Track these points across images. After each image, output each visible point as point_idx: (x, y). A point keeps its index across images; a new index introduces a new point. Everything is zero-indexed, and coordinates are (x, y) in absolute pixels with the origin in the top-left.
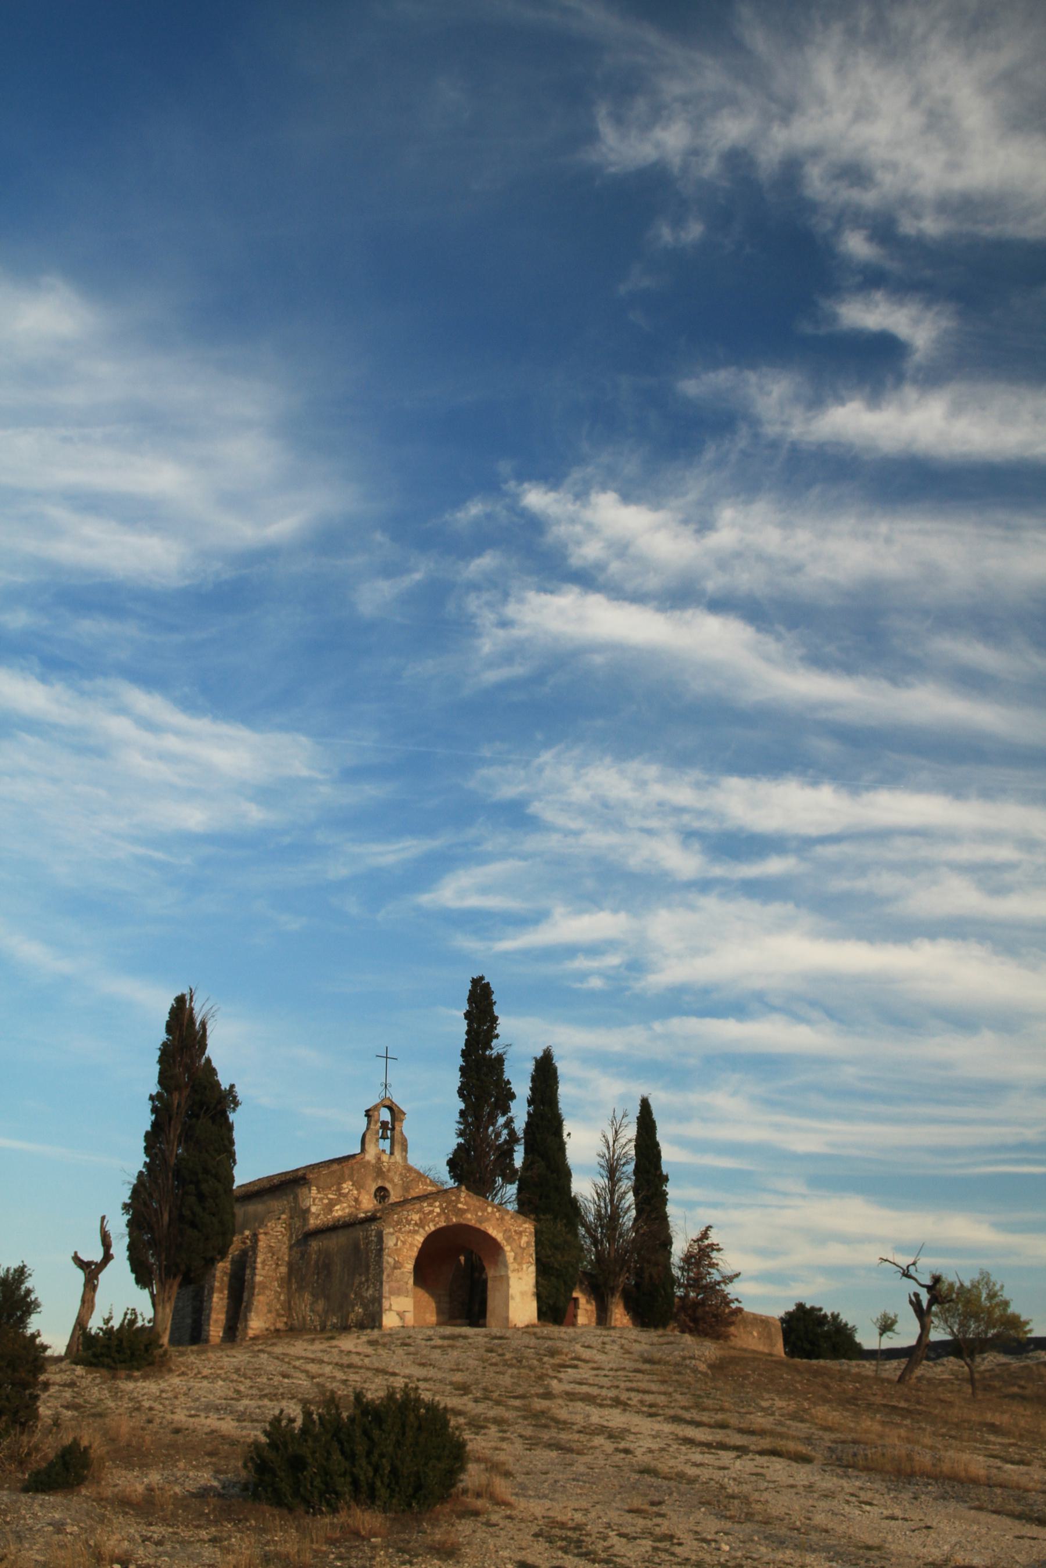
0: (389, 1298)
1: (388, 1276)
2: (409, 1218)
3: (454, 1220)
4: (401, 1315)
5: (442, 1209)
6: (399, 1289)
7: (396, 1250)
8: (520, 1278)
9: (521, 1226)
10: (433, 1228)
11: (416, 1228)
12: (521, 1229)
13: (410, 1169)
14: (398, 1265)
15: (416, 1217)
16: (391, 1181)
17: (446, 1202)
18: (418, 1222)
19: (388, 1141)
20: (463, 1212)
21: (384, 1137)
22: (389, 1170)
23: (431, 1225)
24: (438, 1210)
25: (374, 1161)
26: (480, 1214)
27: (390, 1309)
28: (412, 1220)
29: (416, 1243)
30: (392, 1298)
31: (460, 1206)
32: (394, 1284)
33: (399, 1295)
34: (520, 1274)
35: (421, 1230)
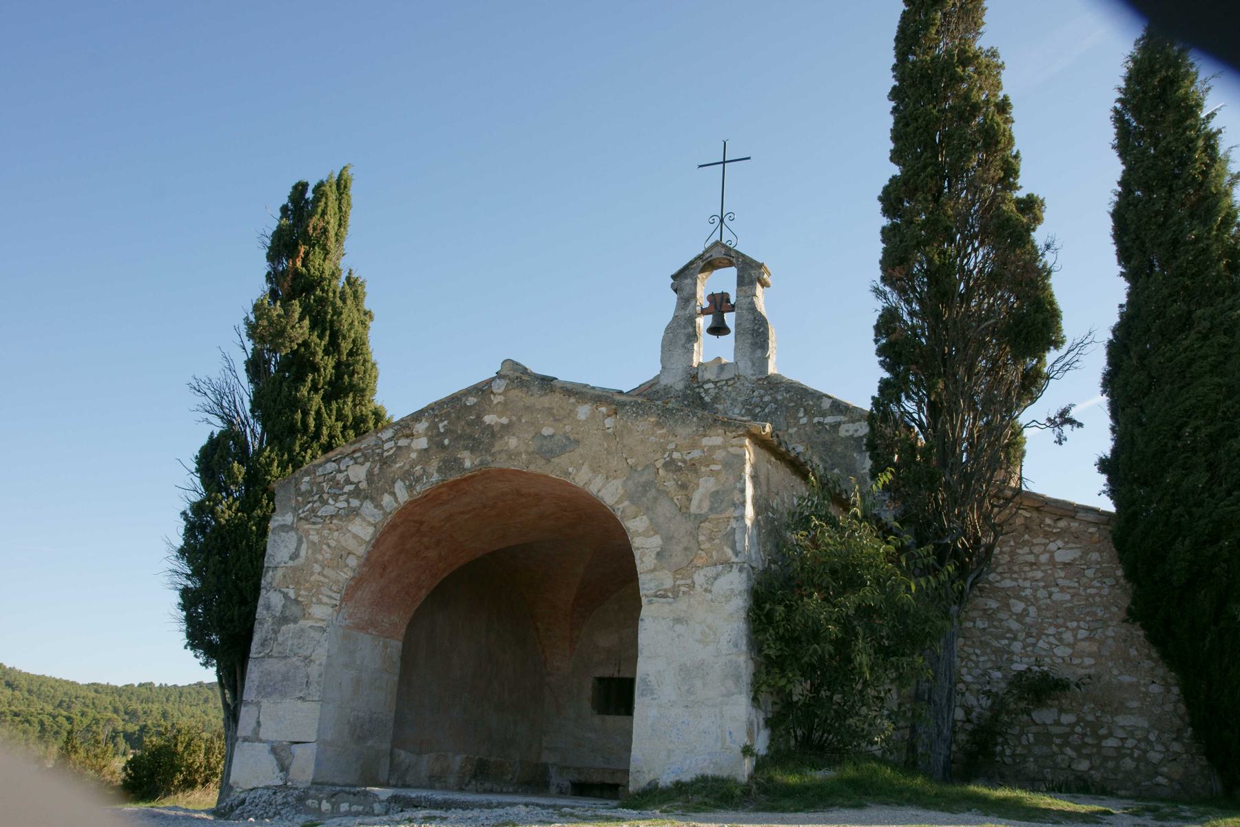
0: (258, 704)
1: (263, 644)
3: (468, 464)
4: (281, 754)
6: (285, 678)
7: (294, 569)
8: (678, 620)
9: (694, 446)
10: (403, 495)
11: (355, 503)
12: (696, 454)
13: (775, 384)
14: (295, 610)
15: (358, 473)
17: (447, 416)
18: (363, 485)
19: (731, 336)
20: (494, 433)
21: (718, 329)
22: (716, 399)
23: (399, 487)
24: (422, 443)
25: (680, 386)
26: (547, 431)
27: (255, 738)
28: (348, 481)
29: (351, 544)
30: (265, 703)
31: (489, 419)
32: (275, 666)
33: (284, 695)
34: (682, 605)
35: (368, 507)
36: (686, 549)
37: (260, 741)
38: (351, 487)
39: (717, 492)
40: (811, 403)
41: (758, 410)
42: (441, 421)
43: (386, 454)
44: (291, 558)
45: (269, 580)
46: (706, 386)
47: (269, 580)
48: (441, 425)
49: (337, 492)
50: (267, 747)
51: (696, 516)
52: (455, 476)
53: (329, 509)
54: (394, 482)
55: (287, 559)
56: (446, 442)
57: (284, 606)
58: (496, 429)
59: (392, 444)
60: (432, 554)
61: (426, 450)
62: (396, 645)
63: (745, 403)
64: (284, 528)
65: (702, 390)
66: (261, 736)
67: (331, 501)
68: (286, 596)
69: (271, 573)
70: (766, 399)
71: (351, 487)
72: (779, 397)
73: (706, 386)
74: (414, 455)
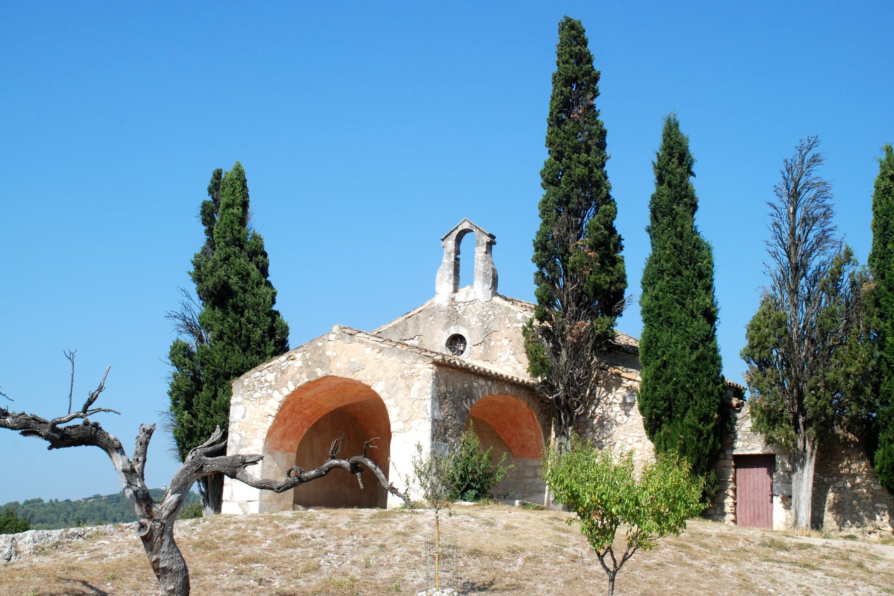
2: (263, 379)
5: (305, 360)
11: (270, 391)
15: (271, 377)
16: (468, 326)
22: (464, 312)
25: (446, 304)
27: (231, 500)
28: (266, 381)
36: (409, 412)
37: (233, 501)
38: (268, 384)
39: (421, 388)
40: (512, 316)
41: (485, 319)
42: (307, 353)
43: (283, 368)
44: (242, 418)
45: (232, 428)
46: (459, 305)
47: (232, 428)
48: (307, 355)
49: (262, 386)
50: (237, 503)
51: (412, 398)
52: (313, 379)
53: (257, 395)
54: (287, 382)
55: (240, 418)
56: (310, 363)
57: (240, 440)
58: (331, 358)
59: (285, 364)
60: (308, 412)
61: (301, 367)
62: (293, 456)
63: (479, 315)
64: (237, 403)
65: (457, 307)
66: (233, 499)
67: (259, 390)
68: (240, 435)
69: (232, 425)
70: (490, 313)
71: (268, 384)
72: (496, 312)
73: (459, 305)
74: (296, 369)
